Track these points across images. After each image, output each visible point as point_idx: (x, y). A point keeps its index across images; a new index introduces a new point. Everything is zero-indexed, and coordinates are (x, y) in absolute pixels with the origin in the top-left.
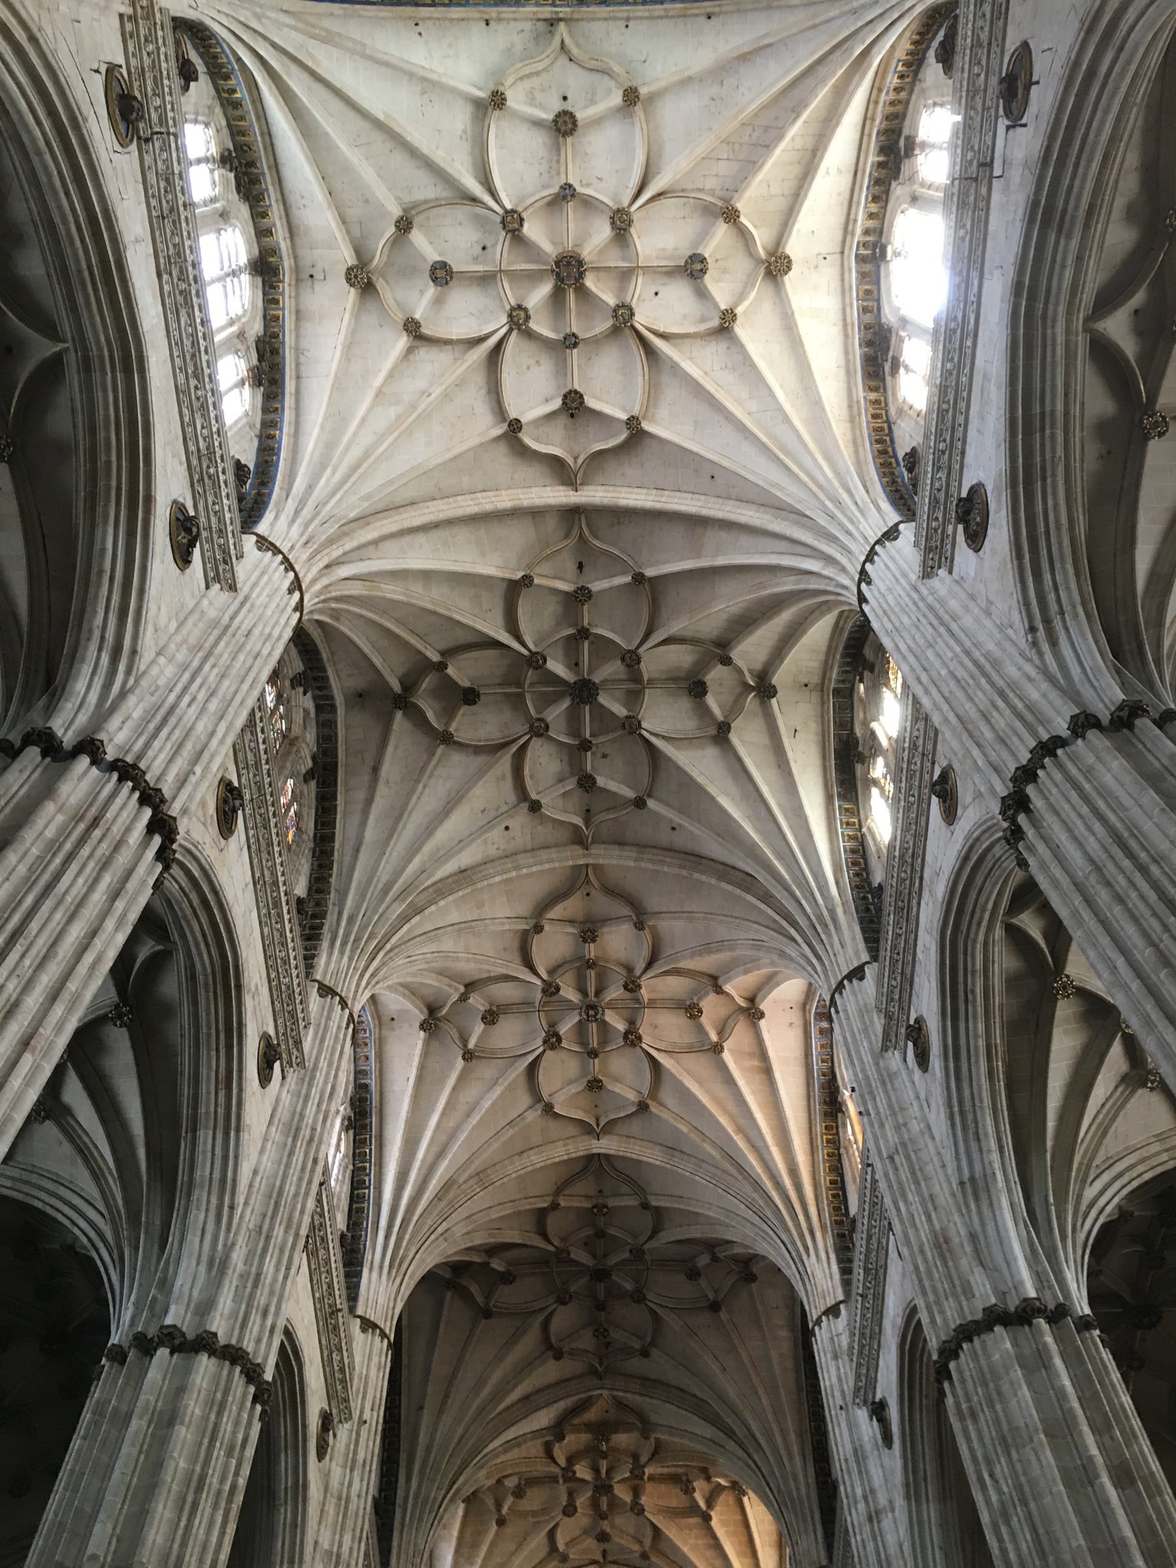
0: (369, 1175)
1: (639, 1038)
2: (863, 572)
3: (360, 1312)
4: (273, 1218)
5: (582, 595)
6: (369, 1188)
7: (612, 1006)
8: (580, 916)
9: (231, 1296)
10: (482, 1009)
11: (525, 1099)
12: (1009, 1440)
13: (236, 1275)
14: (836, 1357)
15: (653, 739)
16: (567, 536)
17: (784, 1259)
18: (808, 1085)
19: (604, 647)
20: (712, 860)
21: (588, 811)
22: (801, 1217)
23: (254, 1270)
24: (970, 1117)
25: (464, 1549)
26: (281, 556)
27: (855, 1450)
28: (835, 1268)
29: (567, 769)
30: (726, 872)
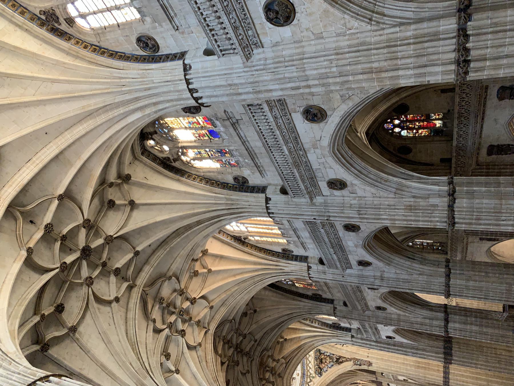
1: (195, 298)
2: (191, 91)
7: (182, 304)
8: (152, 302)
10: (165, 359)
11: (194, 353)
12: (498, 211)
14: (324, 273)
15: (119, 234)
16: (16, 219)
17: (275, 279)
18: (232, 246)
19: (74, 232)
20: (168, 237)
21: (123, 278)
22: (271, 267)
24: (379, 180)
27: (358, 277)
28: (294, 263)
29: (107, 279)
30: (177, 233)
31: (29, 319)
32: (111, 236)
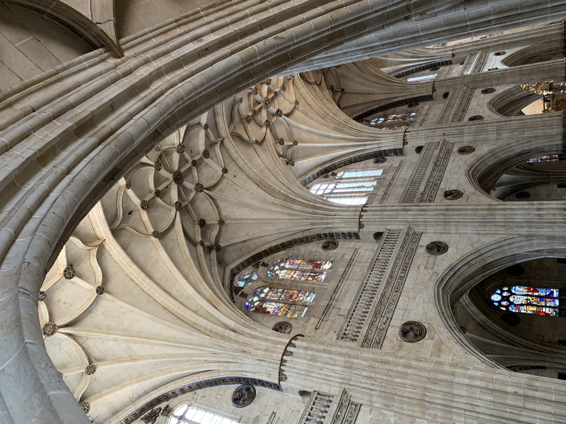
0: (346, 160)
3: (402, 147)
4: (494, 222)
5: (146, 206)
6: (351, 158)
7: (261, 95)
8: (242, 126)
9: (542, 230)
10: (281, 146)
11: (297, 113)
13: (531, 230)
16: (123, 229)
19: (158, 180)
23: (525, 224)
25: (384, 64)
26: (282, 368)
31: (197, 254)
32: (180, 144)
